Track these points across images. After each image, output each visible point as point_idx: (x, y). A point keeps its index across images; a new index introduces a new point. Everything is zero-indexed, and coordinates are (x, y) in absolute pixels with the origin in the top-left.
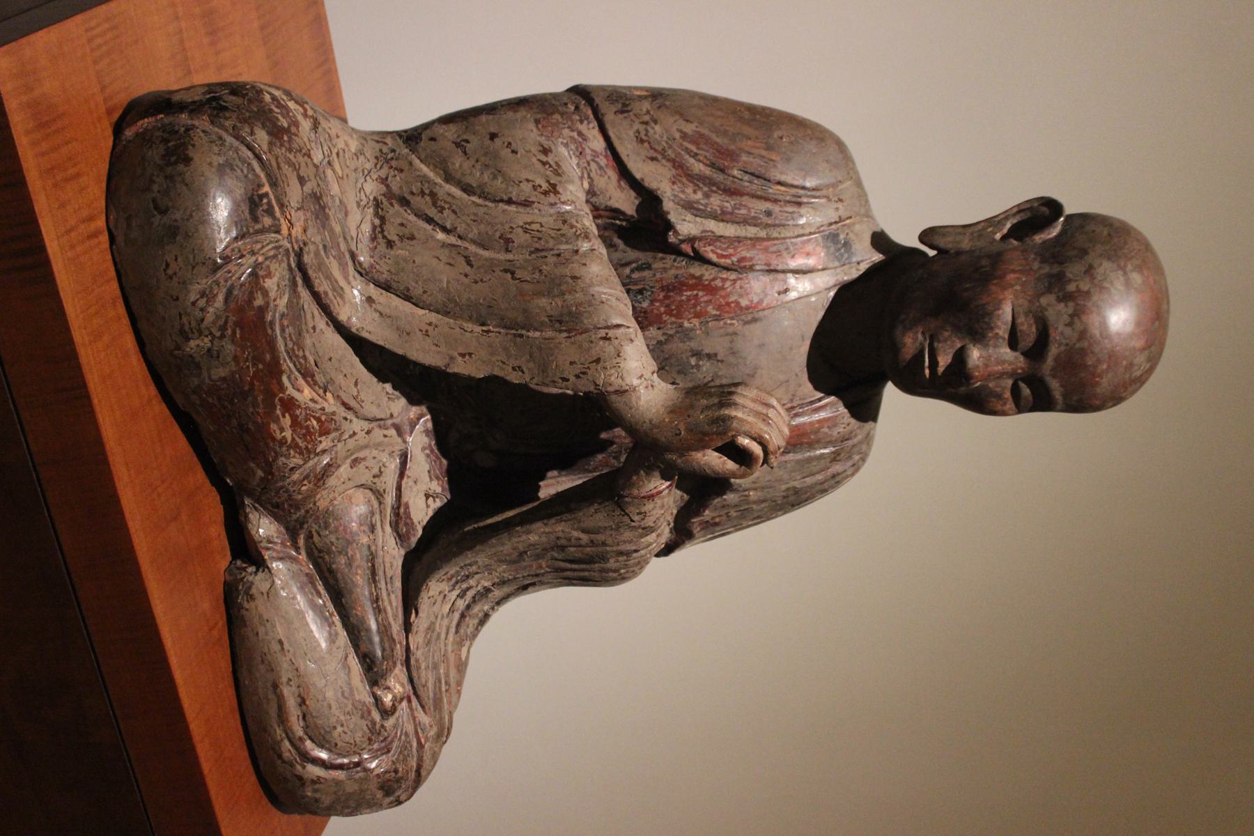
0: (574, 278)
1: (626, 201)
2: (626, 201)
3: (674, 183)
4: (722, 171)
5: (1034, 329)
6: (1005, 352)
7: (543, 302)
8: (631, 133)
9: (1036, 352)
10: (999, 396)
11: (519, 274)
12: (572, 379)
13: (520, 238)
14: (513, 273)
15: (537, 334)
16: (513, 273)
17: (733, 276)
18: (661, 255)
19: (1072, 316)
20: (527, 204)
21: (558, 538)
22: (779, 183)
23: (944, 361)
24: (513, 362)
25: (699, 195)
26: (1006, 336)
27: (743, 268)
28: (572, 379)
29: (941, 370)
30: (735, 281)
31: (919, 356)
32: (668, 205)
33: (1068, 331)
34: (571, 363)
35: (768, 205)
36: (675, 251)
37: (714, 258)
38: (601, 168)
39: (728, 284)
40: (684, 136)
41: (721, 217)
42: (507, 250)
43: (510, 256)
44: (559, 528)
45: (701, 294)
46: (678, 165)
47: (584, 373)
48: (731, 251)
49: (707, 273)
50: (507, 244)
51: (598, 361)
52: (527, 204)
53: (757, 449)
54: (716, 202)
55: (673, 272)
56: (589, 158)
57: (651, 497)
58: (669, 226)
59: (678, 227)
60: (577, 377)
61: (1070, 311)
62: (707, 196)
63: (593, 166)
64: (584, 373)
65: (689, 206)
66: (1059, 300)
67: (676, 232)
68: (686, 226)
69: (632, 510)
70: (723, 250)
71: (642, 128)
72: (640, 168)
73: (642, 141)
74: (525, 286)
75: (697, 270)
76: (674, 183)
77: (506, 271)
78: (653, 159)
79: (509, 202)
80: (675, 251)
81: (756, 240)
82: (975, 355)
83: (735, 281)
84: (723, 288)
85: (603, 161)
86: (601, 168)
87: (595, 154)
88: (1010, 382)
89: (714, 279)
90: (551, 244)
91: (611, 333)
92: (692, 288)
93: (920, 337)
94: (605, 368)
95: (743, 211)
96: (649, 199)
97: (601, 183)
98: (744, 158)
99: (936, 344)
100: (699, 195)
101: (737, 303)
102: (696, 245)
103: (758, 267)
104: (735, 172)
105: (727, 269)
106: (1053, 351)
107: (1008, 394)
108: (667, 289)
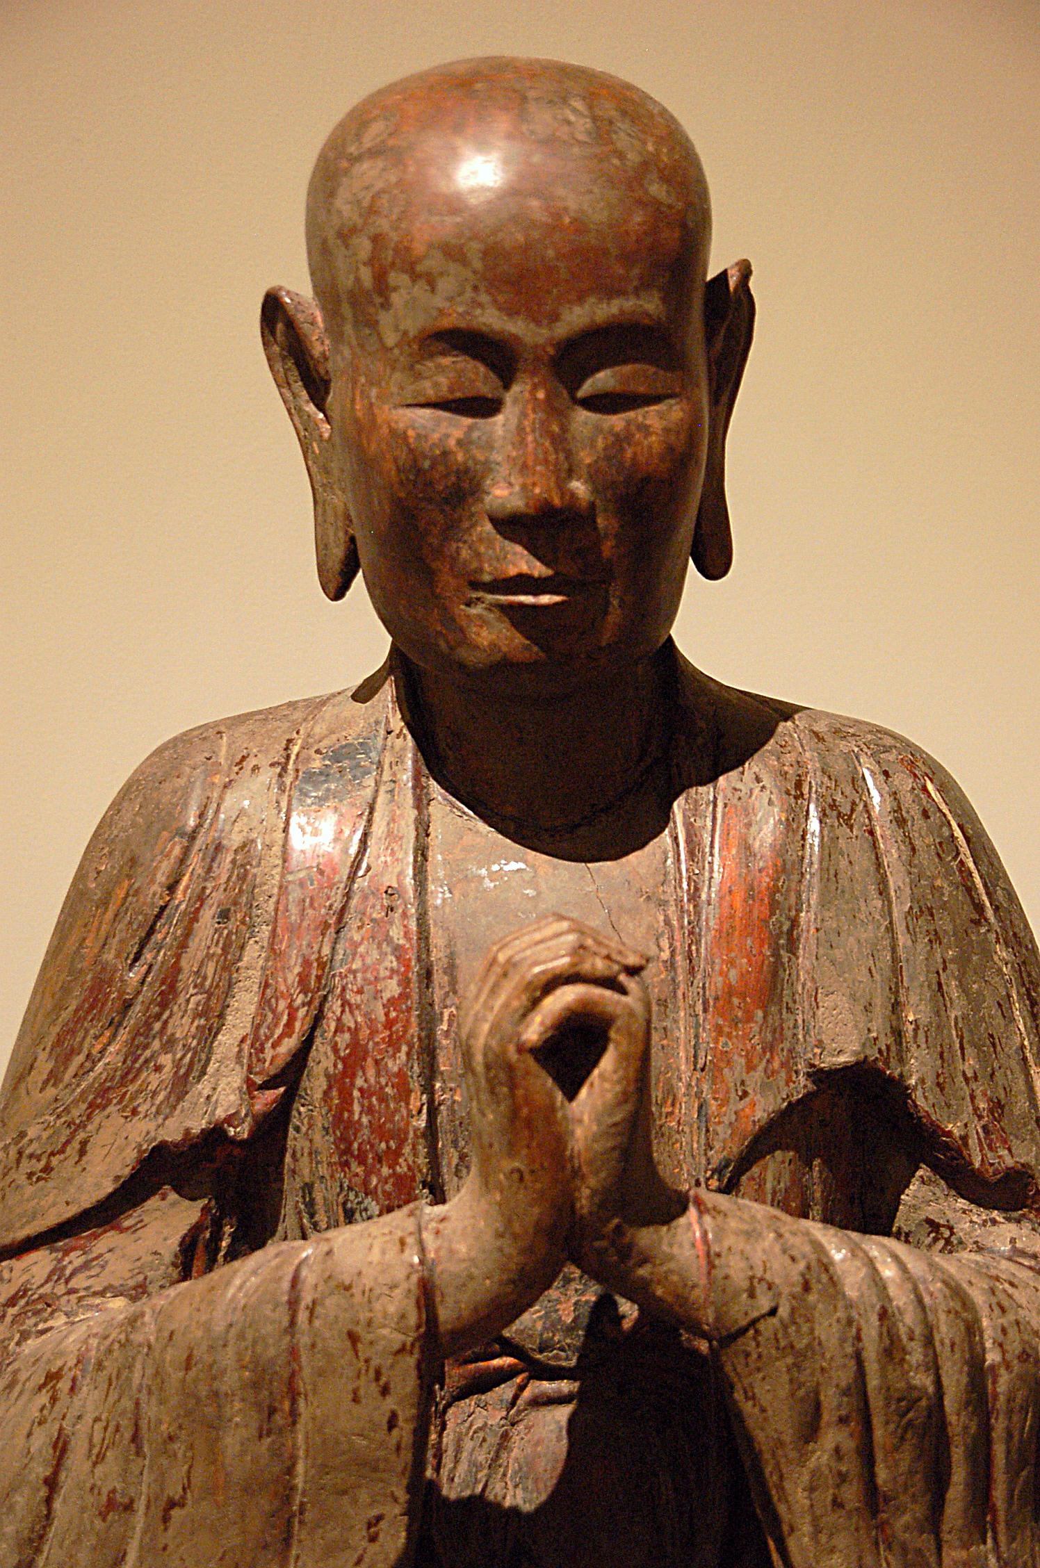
0: (188, 1364)
1: (169, 1219)
2: (169, 1219)
3: (135, 1112)
4: (127, 1005)
5: (446, 361)
6: (500, 424)
7: (231, 1442)
8: (29, 1190)
9: (499, 356)
10: (620, 441)
11: (175, 1491)
12: (390, 1403)
13: (109, 1475)
14: (172, 1504)
15: (300, 1468)
16: (172, 1504)
17: (335, 1006)
18: (288, 1159)
19: (415, 277)
20: (61, 1447)
21: (837, 1504)
22: (172, 888)
23: (521, 561)
24: (358, 1538)
25: (166, 1060)
26: (467, 421)
27: (318, 982)
28: (390, 1403)
29: (539, 569)
30: (345, 1003)
31: (513, 613)
32: (172, 1132)
33: (446, 285)
34: (356, 1400)
35: (208, 915)
36: (273, 1126)
37: (290, 1044)
38: (86, 1266)
39: (348, 1020)
40: (53, 1078)
41: (212, 1019)
42: (129, 1507)
43: (141, 1506)
44: (798, 1496)
45: (359, 1082)
46: (100, 1099)
47: (378, 1374)
48: (282, 1005)
49: (323, 1061)
50: (117, 1506)
51: (353, 1338)
52: (61, 1447)
53: (567, 996)
54: (182, 1025)
55: (317, 1136)
56: (61, 1289)
57: (711, 1259)
58: (215, 1134)
59: (220, 1113)
60: (385, 1391)
61: (405, 279)
62: (169, 1045)
63: (79, 1282)
64: (378, 1374)
65: (181, 1085)
66: (386, 305)
67: (229, 1120)
68: (223, 1097)
69: (740, 1312)
70: (277, 1018)
71: (26, 1166)
72: (97, 1179)
73: (48, 1169)
74: (197, 1480)
75: (315, 1084)
76: (135, 1112)
77: (166, 1519)
78: (82, 1152)
79: (52, 1483)
80: (273, 1126)
81: (273, 951)
82: (504, 493)
83: (345, 1003)
84: (355, 1032)
85: (76, 1259)
86: (86, 1266)
87: (57, 1274)
88: (583, 418)
89: (335, 1050)
90: (127, 1404)
91: (307, 1298)
92: (346, 1100)
93: (475, 611)
94: (369, 1323)
95: (210, 969)
96: (157, 1171)
97: (118, 1270)
98: (109, 956)
99: (487, 578)
100: (166, 1060)
101: (392, 1002)
102: (259, 1080)
103: (326, 951)
104: (133, 976)
105: (318, 1019)
106: (491, 319)
107: (617, 421)
108: (346, 1153)
